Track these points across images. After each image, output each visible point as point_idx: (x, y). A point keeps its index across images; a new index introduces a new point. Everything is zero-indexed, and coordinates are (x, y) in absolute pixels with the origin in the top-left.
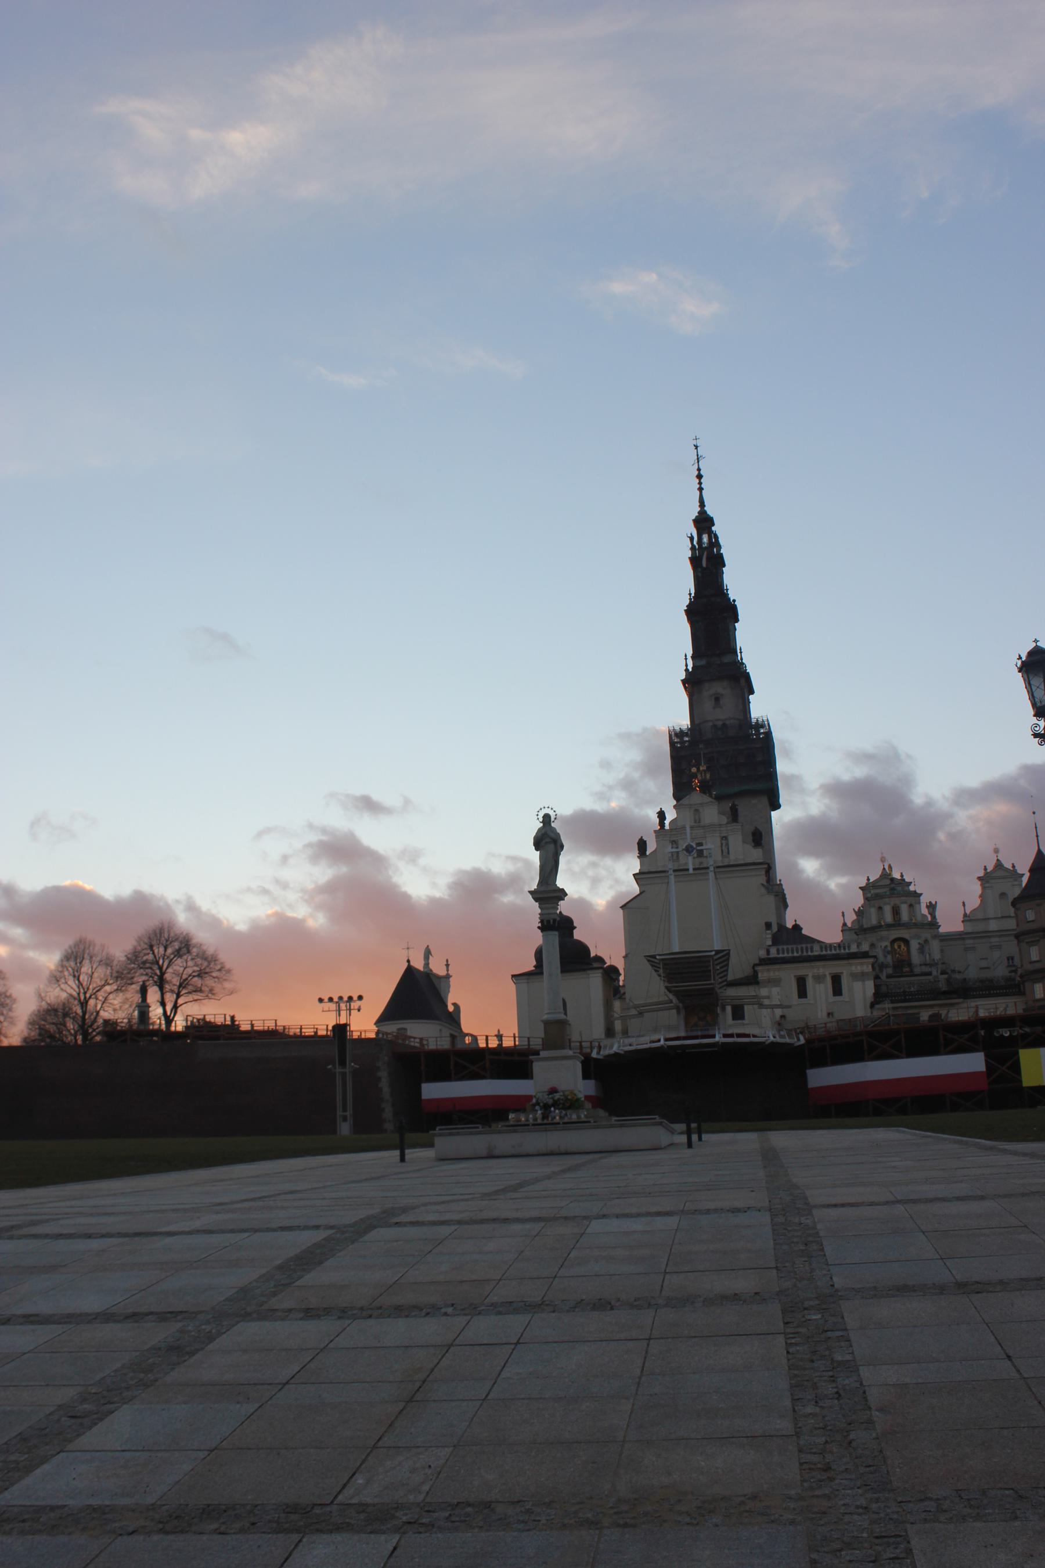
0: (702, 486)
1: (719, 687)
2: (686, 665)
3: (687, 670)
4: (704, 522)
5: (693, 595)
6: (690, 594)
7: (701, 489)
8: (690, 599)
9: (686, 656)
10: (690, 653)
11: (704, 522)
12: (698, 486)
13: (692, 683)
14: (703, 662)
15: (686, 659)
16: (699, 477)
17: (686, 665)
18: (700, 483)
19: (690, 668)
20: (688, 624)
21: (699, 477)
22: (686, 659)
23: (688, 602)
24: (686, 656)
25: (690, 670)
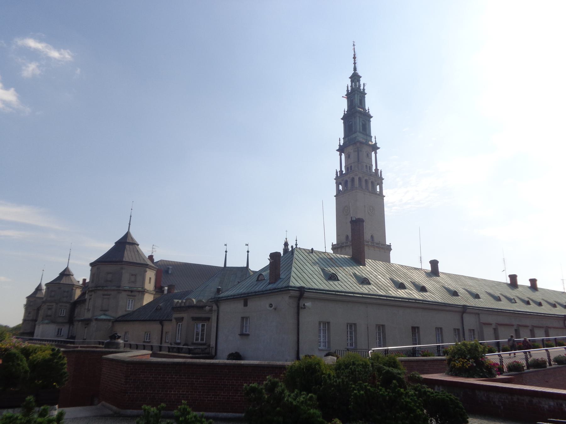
0: (356, 62)
2: (340, 143)
3: (340, 145)
4: (355, 78)
5: (346, 110)
6: (344, 111)
7: (355, 63)
8: (344, 113)
9: (340, 139)
10: (342, 136)
11: (355, 78)
12: (354, 62)
13: (341, 150)
15: (340, 140)
17: (340, 143)
18: (355, 61)
19: (342, 144)
20: (343, 124)
21: (354, 58)
22: (340, 140)
23: (343, 115)
24: (340, 139)
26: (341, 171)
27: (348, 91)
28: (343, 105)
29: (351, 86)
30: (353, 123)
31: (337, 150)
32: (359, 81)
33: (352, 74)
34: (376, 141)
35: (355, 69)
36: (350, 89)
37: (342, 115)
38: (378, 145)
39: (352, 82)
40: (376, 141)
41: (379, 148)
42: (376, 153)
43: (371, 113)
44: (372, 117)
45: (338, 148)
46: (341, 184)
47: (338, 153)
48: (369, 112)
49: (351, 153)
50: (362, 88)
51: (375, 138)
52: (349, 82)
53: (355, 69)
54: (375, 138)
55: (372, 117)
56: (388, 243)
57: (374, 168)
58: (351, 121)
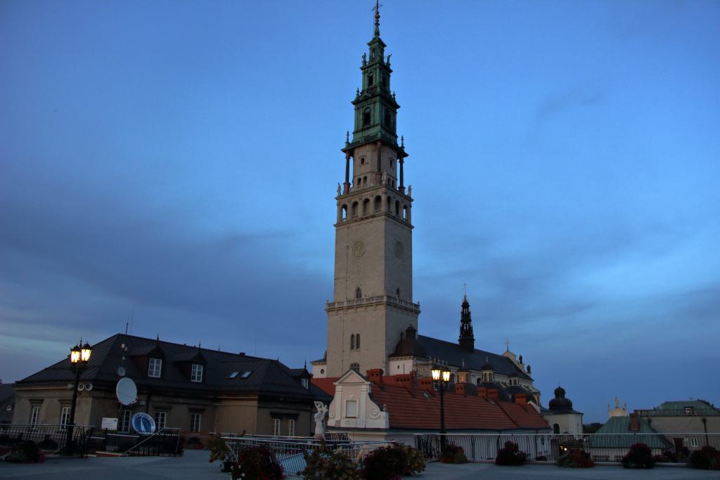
1: (367, 152)
2: (348, 139)
3: (348, 143)
4: (377, 45)
5: (360, 91)
6: (358, 91)
7: (377, 24)
8: (358, 94)
10: (352, 129)
11: (377, 45)
12: (375, 22)
13: (350, 151)
14: (360, 135)
15: (348, 135)
16: (377, 17)
17: (348, 139)
19: (350, 141)
21: (377, 17)
22: (348, 135)
25: (350, 141)
26: (347, 184)
27: (365, 62)
28: (357, 83)
29: (371, 57)
30: (372, 112)
31: (344, 151)
32: (382, 51)
33: (371, 40)
34: (402, 144)
35: (377, 33)
36: (367, 60)
37: (353, 98)
38: (406, 151)
39: (373, 50)
40: (402, 144)
41: (406, 155)
42: (402, 162)
43: (398, 101)
44: (398, 107)
45: (344, 146)
46: (345, 207)
47: (344, 155)
48: (394, 98)
49: (366, 156)
50: (385, 61)
51: (402, 140)
52: (367, 50)
53: (377, 33)
54: (402, 140)
55: (398, 107)
56: (415, 301)
57: (398, 184)
58: (368, 108)
